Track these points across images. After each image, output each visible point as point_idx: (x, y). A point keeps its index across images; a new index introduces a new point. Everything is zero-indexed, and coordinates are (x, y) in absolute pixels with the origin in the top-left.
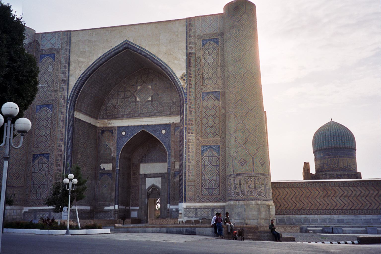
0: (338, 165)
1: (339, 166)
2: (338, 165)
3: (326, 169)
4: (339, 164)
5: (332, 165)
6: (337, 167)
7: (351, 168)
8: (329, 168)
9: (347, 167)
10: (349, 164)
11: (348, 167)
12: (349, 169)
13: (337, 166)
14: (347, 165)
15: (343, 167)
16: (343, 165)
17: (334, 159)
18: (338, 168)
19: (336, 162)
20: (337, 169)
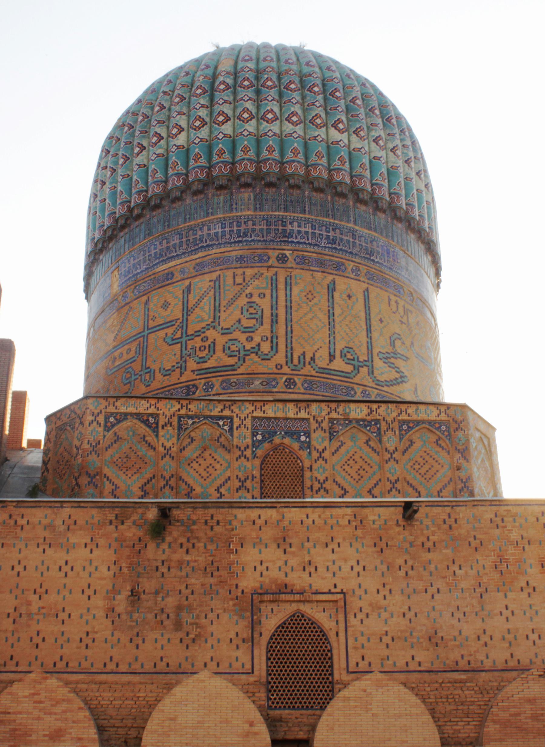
0: (281, 330)
1: (290, 348)
2: (281, 330)
3: (167, 373)
4: (287, 321)
5: (226, 332)
6: (274, 347)
8: (192, 365)
12: (378, 383)
13: (273, 340)
15: (332, 357)
16: (331, 343)
17: (249, 272)
18: (280, 358)
19: (265, 304)
20: (270, 366)
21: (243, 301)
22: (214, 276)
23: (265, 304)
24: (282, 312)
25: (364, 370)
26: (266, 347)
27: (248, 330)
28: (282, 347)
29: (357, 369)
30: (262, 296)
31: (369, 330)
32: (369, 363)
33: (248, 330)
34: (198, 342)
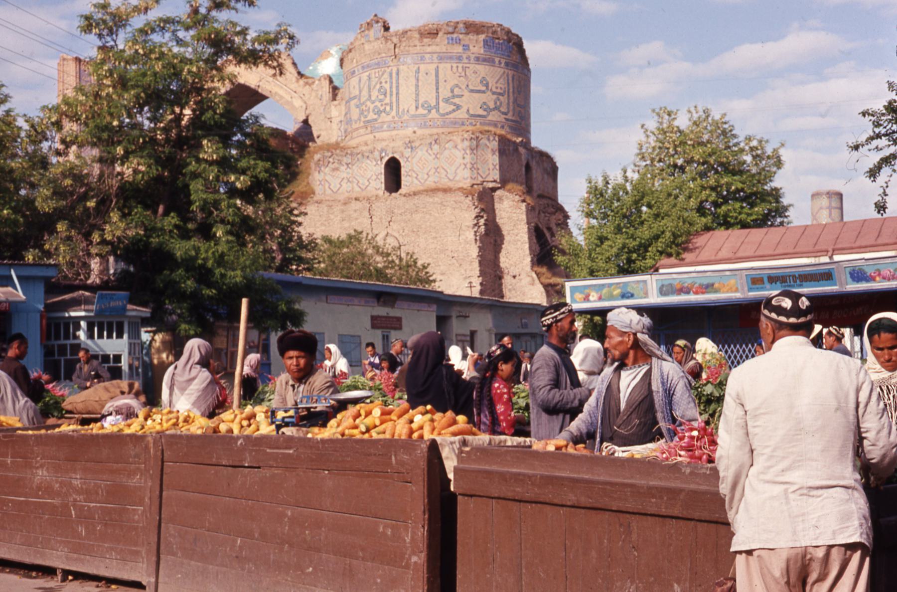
0: (394, 99)
4: (397, 94)
5: (373, 102)
6: (391, 109)
7: (458, 107)
9: (438, 103)
10: (445, 93)
11: (442, 104)
14: (437, 98)
15: (417, 108)
18: (394, 113)
19: (387, 86)
20: (389, 118)
21: (378, 86)
22: (367, 73)
23: (387, 86)
24: (394, 90)
25: (434, 111)
26: (388, 108)
27: (381, 101)
28: (394, 107)
29: (430, 111)
30: (386, 82)
31: (437, 89)
32: (437, 107)
33: (381, 101)
34: (364, 107)
